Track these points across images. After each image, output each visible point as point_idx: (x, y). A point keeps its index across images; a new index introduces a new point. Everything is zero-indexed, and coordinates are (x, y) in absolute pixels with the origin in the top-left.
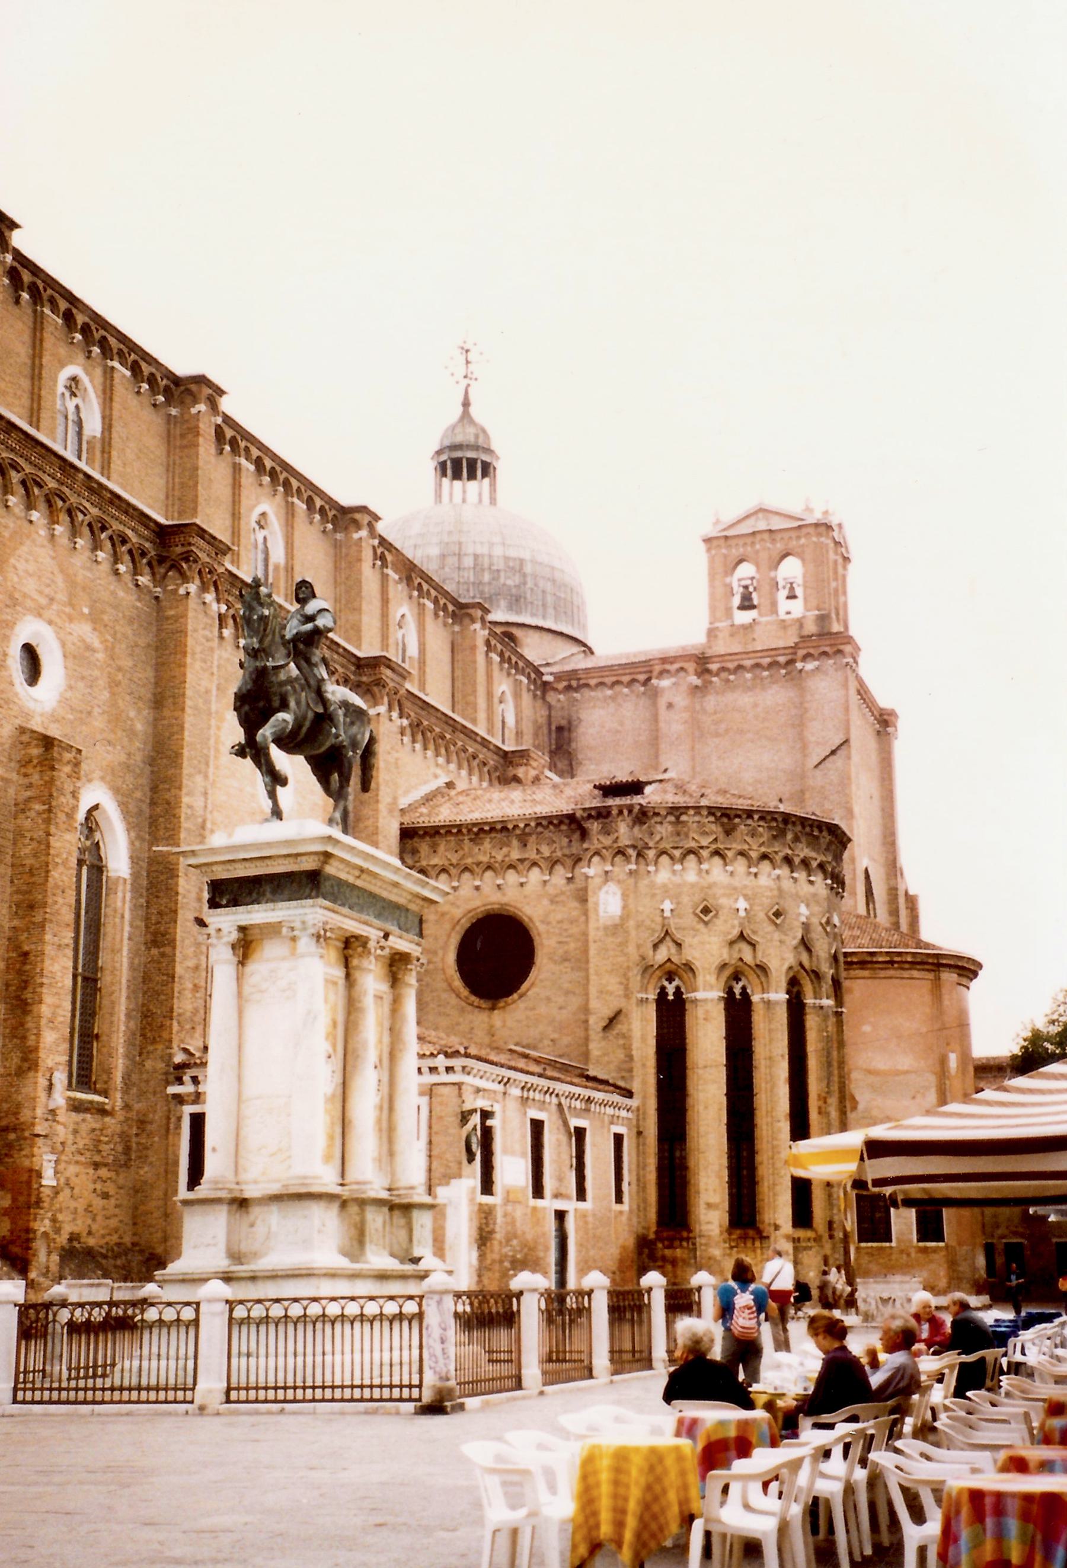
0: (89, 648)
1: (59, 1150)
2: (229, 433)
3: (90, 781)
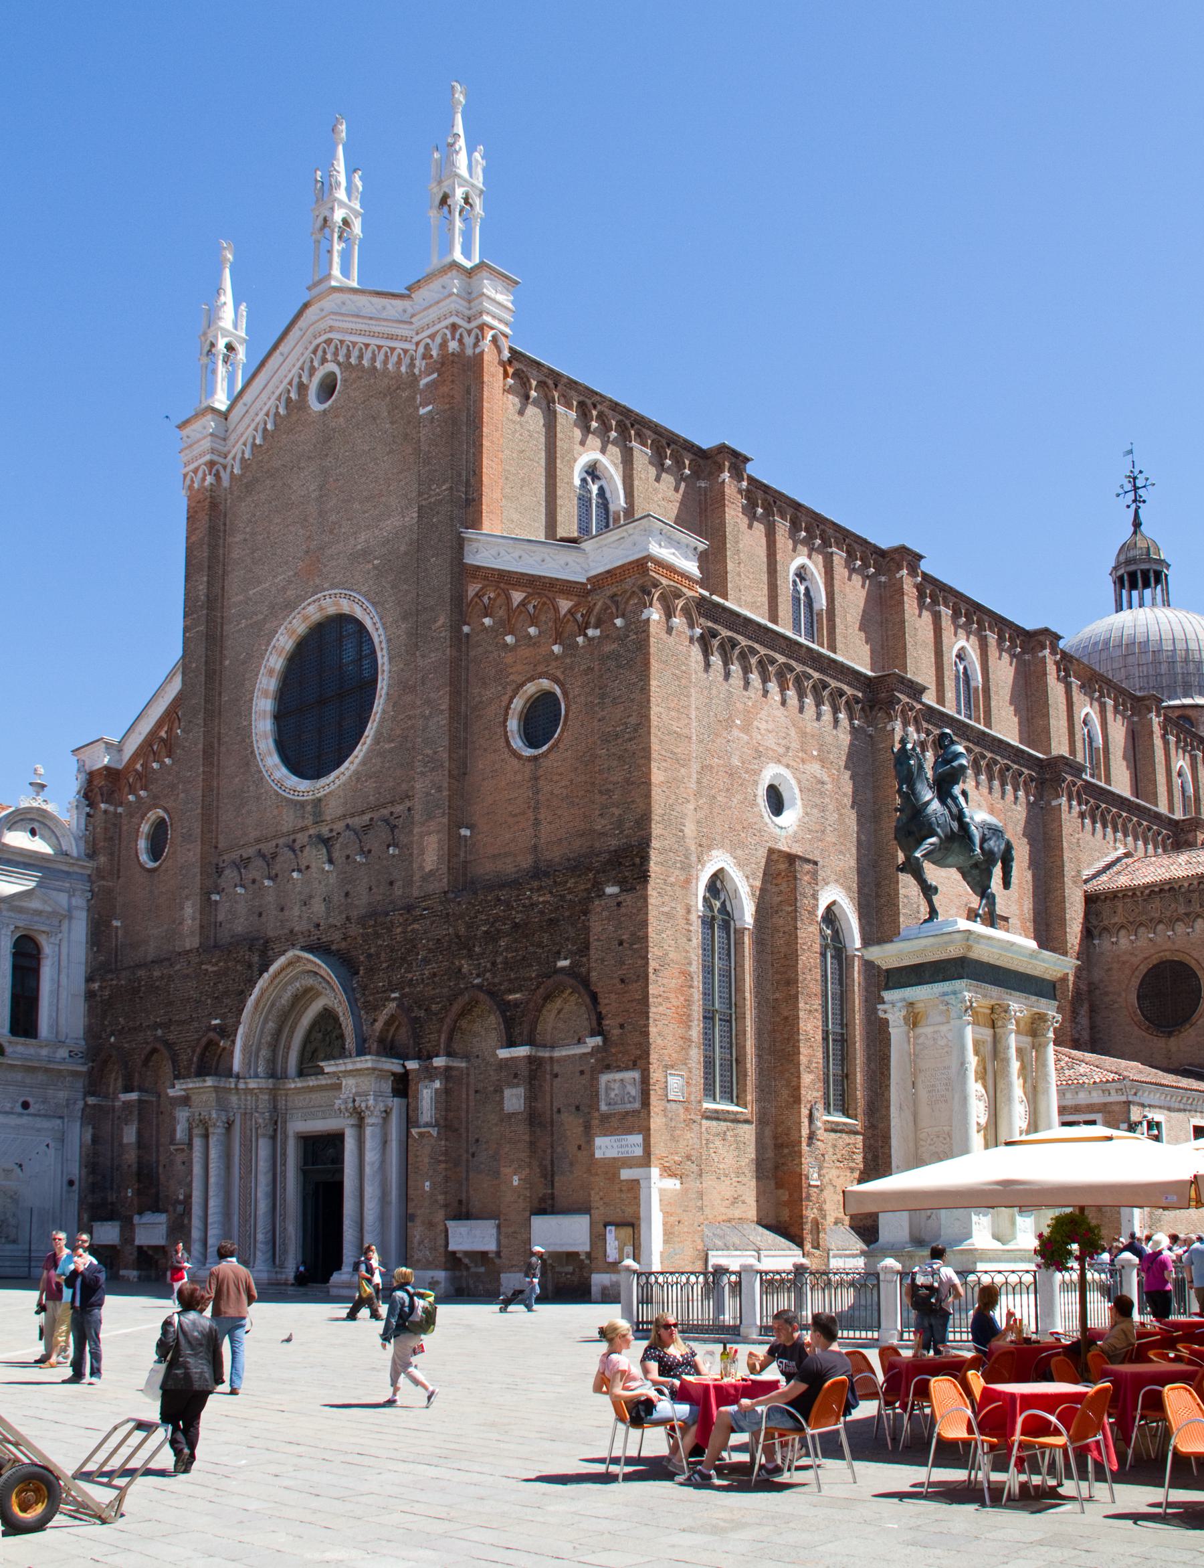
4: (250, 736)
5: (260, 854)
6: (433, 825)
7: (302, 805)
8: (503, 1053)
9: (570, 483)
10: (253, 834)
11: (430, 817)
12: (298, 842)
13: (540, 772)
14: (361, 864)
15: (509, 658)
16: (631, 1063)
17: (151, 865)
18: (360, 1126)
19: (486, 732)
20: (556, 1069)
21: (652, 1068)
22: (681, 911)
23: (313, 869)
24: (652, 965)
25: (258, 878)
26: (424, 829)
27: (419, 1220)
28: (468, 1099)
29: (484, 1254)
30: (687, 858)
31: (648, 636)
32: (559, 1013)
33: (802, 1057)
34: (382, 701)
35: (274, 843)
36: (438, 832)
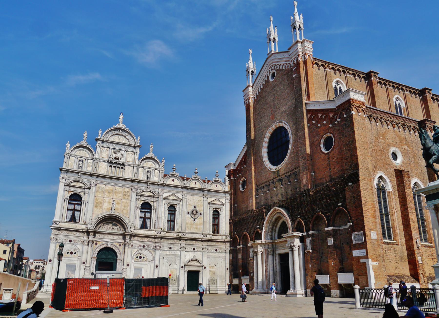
0: (407, 150)
1: (422, 255)
2: (435, 98)
3: (413, 177)
4: (262, 158)
5: (266, 185)
6: (305, 173)
7: (274, 172)
8: (327, 229)
9: (332, 87)
10: (264, 181)
11: (304, 171)
12: (274, 181)
13: (330, 156)
14: (289, 185)
15: (319, 130)
16: (360, 230)
17: (242, 191)
18: (292, 251)
19: (316, 148)
20: (341, 232)
21: (366, 231)
22: (370, 188)
23: (278, 187)
24: (363, 202)
25: (266, 191)
26: (302, 174)
28: (319, 242)
29: (326, 284)
30: (370, 173)
31: (353, 118)
32: (340, 218)
33: (411, 226)
34: (291, 145)
35: (269, 182)
36: (306, 174)
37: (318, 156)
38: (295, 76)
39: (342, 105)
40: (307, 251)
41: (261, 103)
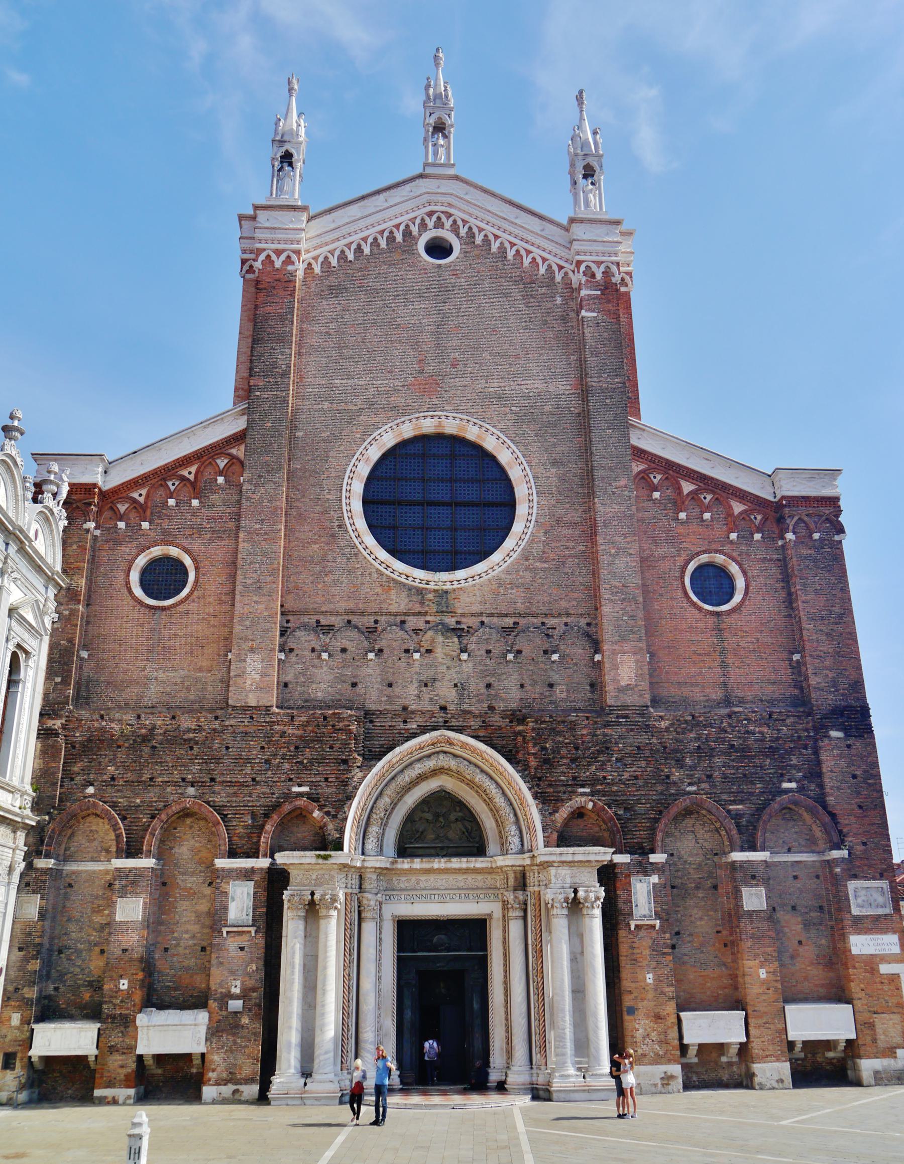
6: (627, 647)
7: (420, 592)
10: (342, 606)
11: (623, 639)
15: (681, 529)
16: (878, 875)
23: (439, 652)
26: (616, 647)
27: (640, 1014)
36: (635, 653)
37: (672, 608)
38: (595, 318)
39: (806, 499)
40: (639, 923)
41: (355, 305)
